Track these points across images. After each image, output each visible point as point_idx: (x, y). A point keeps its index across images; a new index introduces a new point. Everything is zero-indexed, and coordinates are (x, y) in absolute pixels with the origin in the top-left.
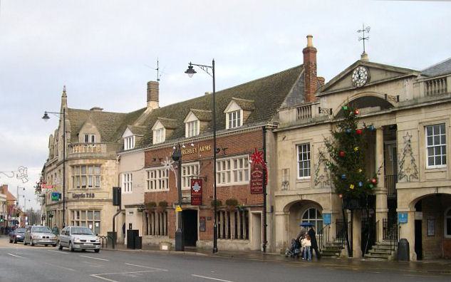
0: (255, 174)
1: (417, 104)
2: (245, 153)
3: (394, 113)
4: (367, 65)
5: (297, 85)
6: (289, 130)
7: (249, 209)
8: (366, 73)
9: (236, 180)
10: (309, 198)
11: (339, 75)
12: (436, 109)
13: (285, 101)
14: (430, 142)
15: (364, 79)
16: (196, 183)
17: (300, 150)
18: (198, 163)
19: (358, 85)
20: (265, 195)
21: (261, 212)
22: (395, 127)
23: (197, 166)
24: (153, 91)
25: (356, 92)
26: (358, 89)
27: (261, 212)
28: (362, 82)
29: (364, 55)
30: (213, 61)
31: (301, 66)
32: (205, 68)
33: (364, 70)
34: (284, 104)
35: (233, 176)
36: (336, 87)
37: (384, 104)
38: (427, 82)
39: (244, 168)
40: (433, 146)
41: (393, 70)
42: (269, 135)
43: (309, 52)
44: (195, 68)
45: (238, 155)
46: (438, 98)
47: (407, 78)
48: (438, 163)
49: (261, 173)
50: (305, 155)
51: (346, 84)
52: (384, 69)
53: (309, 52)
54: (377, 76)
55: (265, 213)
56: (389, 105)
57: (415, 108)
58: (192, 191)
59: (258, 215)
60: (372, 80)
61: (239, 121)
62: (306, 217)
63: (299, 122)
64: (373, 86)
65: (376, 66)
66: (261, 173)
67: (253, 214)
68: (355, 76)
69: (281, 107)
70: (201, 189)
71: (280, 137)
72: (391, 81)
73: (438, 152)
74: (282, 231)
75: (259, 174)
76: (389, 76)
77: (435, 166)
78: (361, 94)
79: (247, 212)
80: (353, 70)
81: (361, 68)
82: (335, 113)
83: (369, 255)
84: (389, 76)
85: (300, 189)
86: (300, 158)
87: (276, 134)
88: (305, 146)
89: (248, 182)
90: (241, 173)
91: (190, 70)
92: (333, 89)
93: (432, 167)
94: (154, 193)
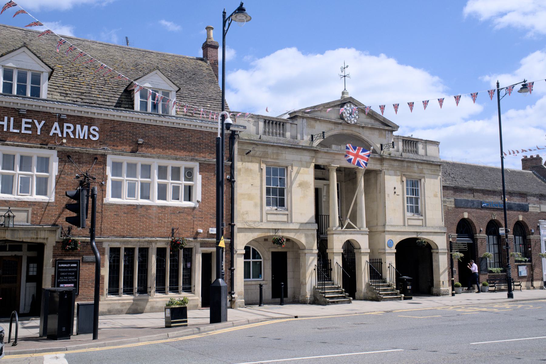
19: (349, 122)
25: (341, 127)
28: (353, 121)
64: (359, 127)
78: (347, 131)
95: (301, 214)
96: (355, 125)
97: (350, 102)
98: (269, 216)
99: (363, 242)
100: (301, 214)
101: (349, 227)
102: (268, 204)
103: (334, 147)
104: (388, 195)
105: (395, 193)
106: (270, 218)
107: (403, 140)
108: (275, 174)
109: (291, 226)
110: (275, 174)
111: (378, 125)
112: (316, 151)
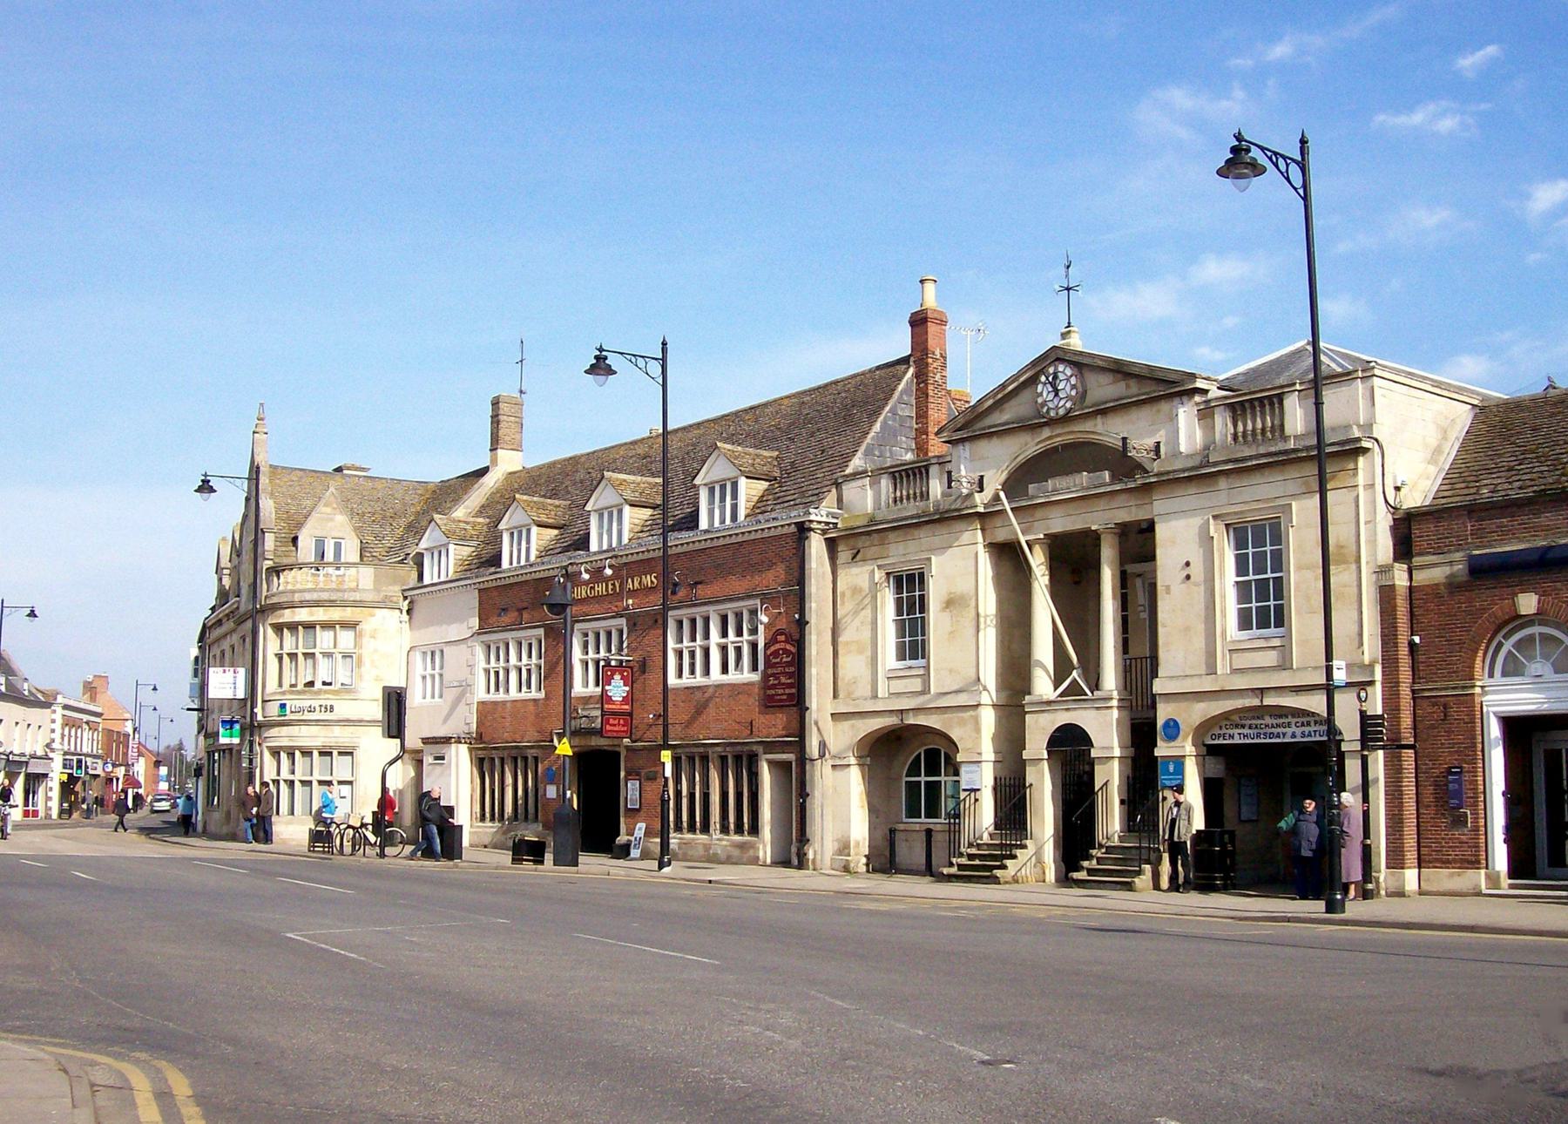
1: (1208, 464)
2: (749, 597)
3: (1147, 489)
4: (1075, 359)
5: (893, 411)
6: (868, 533)
7: (760, 749)
8: (1073, 381)
9: (725, 670)
10: (922, 720)
11: (1003, 386)
12: (1257, 478)
13: (859, 454)
14: (1241, 568)
15: (1069, 398)
16: (617, 677)
17: (899, 589)
18: (623, 621)
19: (1052, 414)
21: (790, 757)
23: (621, 632)
24: (501, 424)
25: (1046, 432)
26: (1051, 422)
30: (664, 344)
31: (904, 361)
32: (641, 362)
33: (1069, 372)
34: (857, 463)
35: (711, 661)
37: (1121, 463)
38: (1232, 407)
39: (746, 636)
40: (1251, 577)
41: (1145, 372)
42: (816, 546)
44: (612, 360)
45: (731, 600)
46: (1262, 450)
47: (1181, 394)
48: (1263, 624)
49: (793, 650)
52: (1120, 370)
54: (1103, 389)
55: (803, 760)
57: (1200, 475)
58: (604, 698)
59: (785, 766)
60: (1089, 400)
61: (734, 508)
62: (914, 770)
65: (1100, 363)
66: (793, 650)
67: (770, 762)
69: (848, 471)
70: (631, 693)
71: (844, 555)
72: (1144, 402)
73: (1263, 595)
74: (844, 807)
75: (786, 651)
76: (1134, 390)
77: (1255, 632)
79: (753, 759)
80: (1042, 371)
81: (1061, 368)
83: (1082, 875)
86: (899, 612)
87: (832, 544)
88: (911, 578)
89: (755, 677)
90: (738, 650)
91: (600, 367)
92: (988, 421)
93: (1245, 634)
94: (504, 703)
95: (951, 671)
96: (1066, 419)
97: (1058, 359)
98: (893, 682)
100: (951, 671)
101: (1074, 690)
104: (1168, 588)
105: (1188, 577)
106: (899, 686)
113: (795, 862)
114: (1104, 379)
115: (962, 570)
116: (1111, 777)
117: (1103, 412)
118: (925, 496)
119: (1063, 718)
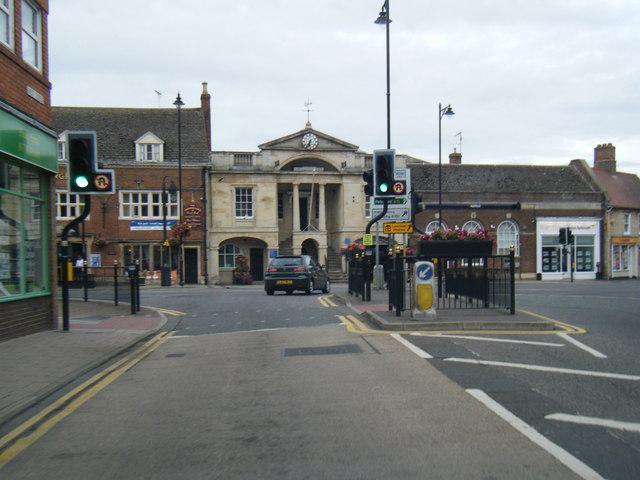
0: (190, 211)
3: (341, 176)
20: (206, 231)
22: (338, 186)
27: (199, 247)
29: (308, 124)
31: (198, 109)
36: (282, 145)
42: (207, 176)
43: (205, 98)
50: (244, 199)
51: (295, 144)
52: (332, 140)
53: (205, 98)
54: (325, 145)
56: (337, 170)
63: (240, 168)
68: (306, 140)
71: (214, 180)
76: (334, 146)
82: (279, 167)
84: (339, 147)
85: (240, 228)
87: (210, 174)
88: (244, 191)
99: (322, 240)
102: (238, 214)
103: (295, 169)
107: (366, 158)
108: (244, 193)
109: (256, 230)
110: (244, 193)
111: (339, 147)
112: (278, 174)
113: (203, 282)
114: (325, 141)
115: (265, 192)
116: (323, 254)
117: (324, 151)
118: (251, 165)
119: (307, 236)
